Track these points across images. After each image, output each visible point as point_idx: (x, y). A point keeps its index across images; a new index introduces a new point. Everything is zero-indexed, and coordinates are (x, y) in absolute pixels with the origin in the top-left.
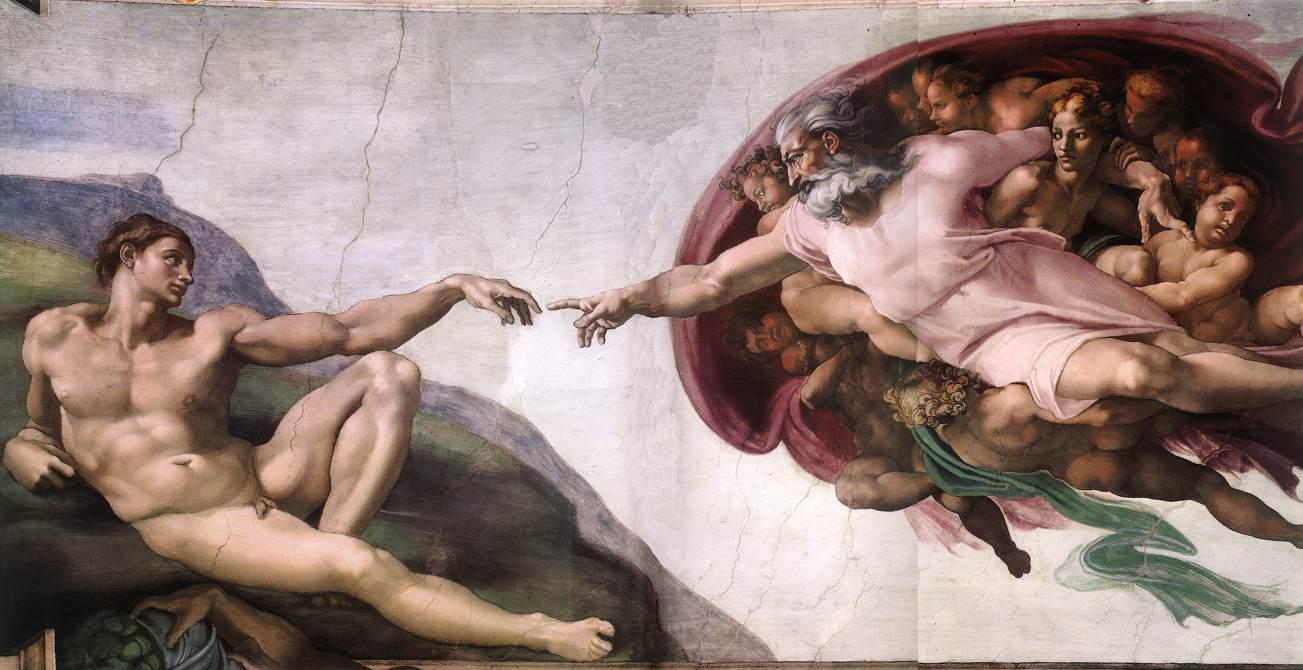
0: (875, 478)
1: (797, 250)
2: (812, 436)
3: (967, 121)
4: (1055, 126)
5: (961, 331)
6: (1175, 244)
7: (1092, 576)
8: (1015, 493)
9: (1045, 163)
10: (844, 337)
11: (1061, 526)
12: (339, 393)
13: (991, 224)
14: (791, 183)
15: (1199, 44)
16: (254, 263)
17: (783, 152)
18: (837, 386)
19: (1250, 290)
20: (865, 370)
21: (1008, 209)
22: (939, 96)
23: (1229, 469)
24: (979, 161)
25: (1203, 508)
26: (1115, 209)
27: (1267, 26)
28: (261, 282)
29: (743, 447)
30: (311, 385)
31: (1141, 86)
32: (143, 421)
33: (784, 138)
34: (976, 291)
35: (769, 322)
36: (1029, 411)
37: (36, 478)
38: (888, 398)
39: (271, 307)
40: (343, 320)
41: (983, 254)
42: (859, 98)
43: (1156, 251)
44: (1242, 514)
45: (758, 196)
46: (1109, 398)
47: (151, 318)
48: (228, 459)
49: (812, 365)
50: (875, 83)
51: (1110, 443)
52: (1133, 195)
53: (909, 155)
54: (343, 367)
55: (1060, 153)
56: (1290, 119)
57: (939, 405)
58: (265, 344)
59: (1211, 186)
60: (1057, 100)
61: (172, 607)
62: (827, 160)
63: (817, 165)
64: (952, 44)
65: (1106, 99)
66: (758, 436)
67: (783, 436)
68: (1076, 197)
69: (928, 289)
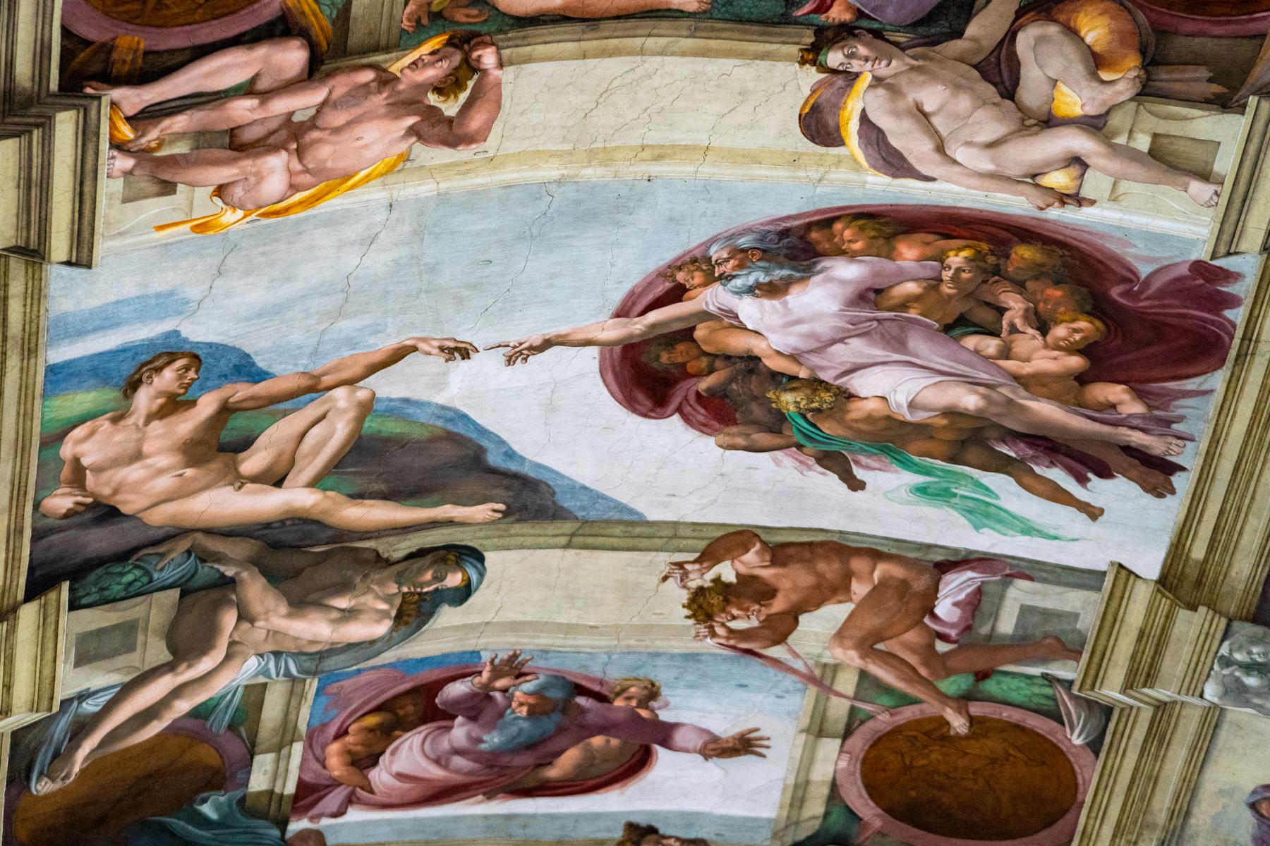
0: (749, 435)
1: (712, 309)
2: (703, 411)
3: (874, 251)
4: (946, 262)
5: (840, 364)
6: (1028, 341)
7: (912, 497)
8: (862, 451)
9: (934, 282)
10: (741, 358)
11: (896, 472)
12: (311, 412)
13: (879, 309)
14: (716, 275)
15: (1080, 241)
16: (248, 355)
17: (714, 259)
18: (730, 383)
19: (1083, 379)
20: (754, 377)
21: (892, 302)
22: (853, 235)
23: (1037, 464)
24: (876, 275)
25: (1011, 479)
26: (984, 315)
27: (1140, 244)
28: (253, 364)
29: (645, 416)
30: (285, 414)
31: (1024, 253)
32: (149, 461)
33: (716, 252)
34: (856, 343)
35: (681, 347)
36: (887, 412)
37: (64, 511)
38: (770, 395)
39: (259, 376)
40: (315, 373)
41: (869, 324)
42: (785, 233)
43: (1011, 342)
44: (1041, 488)
45: (687, 281)
46: (951, 413)
47: (162, 407)
48: (216, 465)
49: (711, 371)
50: (799, 227)
51: (950, 436)
52: (1001, 311)
53: (819, 267)
54: (313, 400)
55: (944, 278)
56: (1143, 297)
57: (813, 402)
58: (252, 398)
59: (1066, 318)
60: (951, 250)
61: (161, 549)
62: (749, 264)
63: (741, 266)
64: (871, 209)
65: (993, 254)
66: (658, 410)
67: (679, 410)
68: (954, 302)
69: (819, 340)
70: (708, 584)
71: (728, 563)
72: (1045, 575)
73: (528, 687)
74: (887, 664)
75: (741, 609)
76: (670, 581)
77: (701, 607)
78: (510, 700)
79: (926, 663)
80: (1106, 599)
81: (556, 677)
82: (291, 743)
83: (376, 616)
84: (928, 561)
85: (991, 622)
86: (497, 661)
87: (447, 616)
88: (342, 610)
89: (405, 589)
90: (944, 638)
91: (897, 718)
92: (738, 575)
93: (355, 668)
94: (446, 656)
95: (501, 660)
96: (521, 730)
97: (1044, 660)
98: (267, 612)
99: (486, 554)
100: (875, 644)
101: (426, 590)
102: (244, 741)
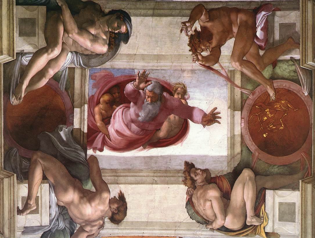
70: (193, 33)
71: (197, 21)
72: (283, 7)
73: (149, 87)
74: (248, 67)
75: (204, 46)
76: (183, 31)
77: (193, 45)
78: (145, 94)
79: (259, 64)
80: (301, 12)
81: (156, 82)
82: (84, 104)
83: (103, 42)
84: (251, 10)
85: (273, 36)
86: (140, 74)
87: (124, 48)
88: (93, 35)
89: (110, 30)
90: (260, 47)
91: (255, 96)
92: (201, 27)
93: (99, 67)
94: (125, 69)
95: (141, 74)
96: (150, 110)
97: (289, 51)
98: (72, 29)
99: (132, 18)
100: (243, 58)
101: (116, 32)
102: (70, 97)
